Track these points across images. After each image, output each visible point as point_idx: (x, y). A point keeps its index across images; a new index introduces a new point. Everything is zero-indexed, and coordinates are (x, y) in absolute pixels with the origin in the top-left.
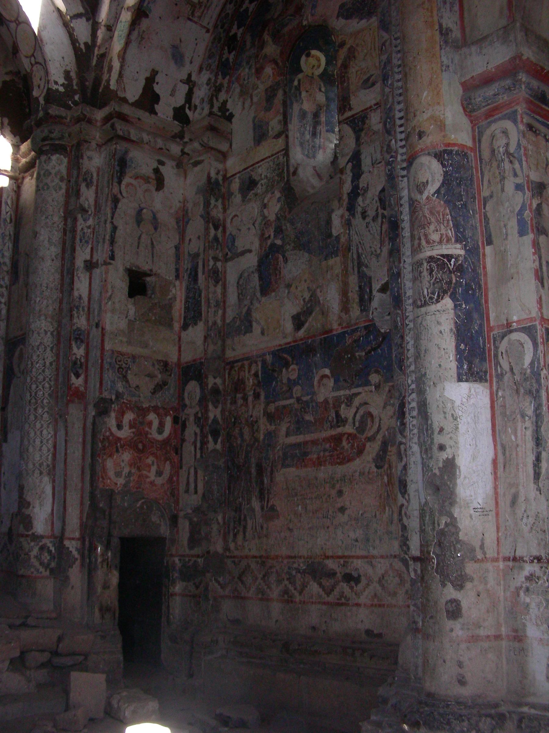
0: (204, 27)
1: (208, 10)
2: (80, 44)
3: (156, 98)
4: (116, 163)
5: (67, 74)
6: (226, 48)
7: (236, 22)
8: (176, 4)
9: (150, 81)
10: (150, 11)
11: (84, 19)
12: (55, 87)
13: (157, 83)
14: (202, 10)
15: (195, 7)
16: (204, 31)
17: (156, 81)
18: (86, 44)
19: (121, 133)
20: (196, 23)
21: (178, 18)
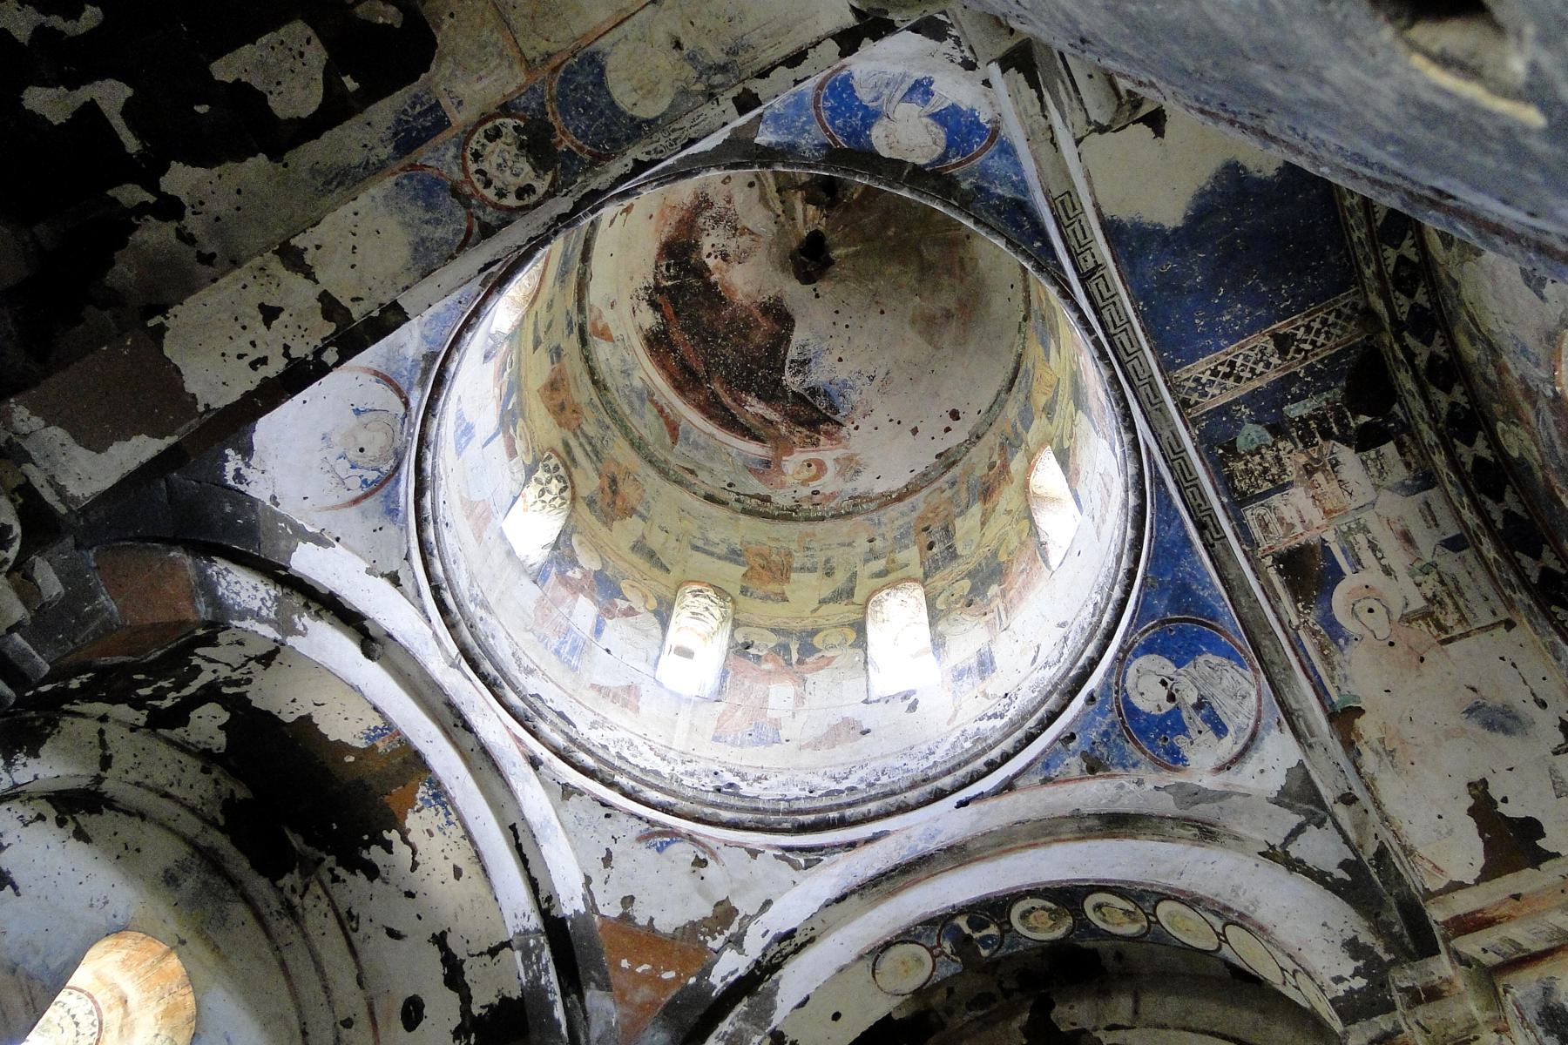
0: (1494, 626)
1: (1462, 595)
2: (1330, 874)
3: (1531, 828)
4: (1540, 1031)
5: (1354, 947)
6: (1554, 608)
7: (1517, 554)
8: (1391, 644)
9: (1484, 808)
10: (1356, 698)
11: (1312, 829)
12: (1341, 990)
13: (1505, 800)
14: (1451, 607)
15: (1431, 614)
16: (1501, 630)
17: (1498, 799)
18: (1344, 865)
19: (1491, 959)
20: (1467, 635)
21: (1422, 660)
